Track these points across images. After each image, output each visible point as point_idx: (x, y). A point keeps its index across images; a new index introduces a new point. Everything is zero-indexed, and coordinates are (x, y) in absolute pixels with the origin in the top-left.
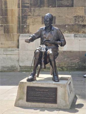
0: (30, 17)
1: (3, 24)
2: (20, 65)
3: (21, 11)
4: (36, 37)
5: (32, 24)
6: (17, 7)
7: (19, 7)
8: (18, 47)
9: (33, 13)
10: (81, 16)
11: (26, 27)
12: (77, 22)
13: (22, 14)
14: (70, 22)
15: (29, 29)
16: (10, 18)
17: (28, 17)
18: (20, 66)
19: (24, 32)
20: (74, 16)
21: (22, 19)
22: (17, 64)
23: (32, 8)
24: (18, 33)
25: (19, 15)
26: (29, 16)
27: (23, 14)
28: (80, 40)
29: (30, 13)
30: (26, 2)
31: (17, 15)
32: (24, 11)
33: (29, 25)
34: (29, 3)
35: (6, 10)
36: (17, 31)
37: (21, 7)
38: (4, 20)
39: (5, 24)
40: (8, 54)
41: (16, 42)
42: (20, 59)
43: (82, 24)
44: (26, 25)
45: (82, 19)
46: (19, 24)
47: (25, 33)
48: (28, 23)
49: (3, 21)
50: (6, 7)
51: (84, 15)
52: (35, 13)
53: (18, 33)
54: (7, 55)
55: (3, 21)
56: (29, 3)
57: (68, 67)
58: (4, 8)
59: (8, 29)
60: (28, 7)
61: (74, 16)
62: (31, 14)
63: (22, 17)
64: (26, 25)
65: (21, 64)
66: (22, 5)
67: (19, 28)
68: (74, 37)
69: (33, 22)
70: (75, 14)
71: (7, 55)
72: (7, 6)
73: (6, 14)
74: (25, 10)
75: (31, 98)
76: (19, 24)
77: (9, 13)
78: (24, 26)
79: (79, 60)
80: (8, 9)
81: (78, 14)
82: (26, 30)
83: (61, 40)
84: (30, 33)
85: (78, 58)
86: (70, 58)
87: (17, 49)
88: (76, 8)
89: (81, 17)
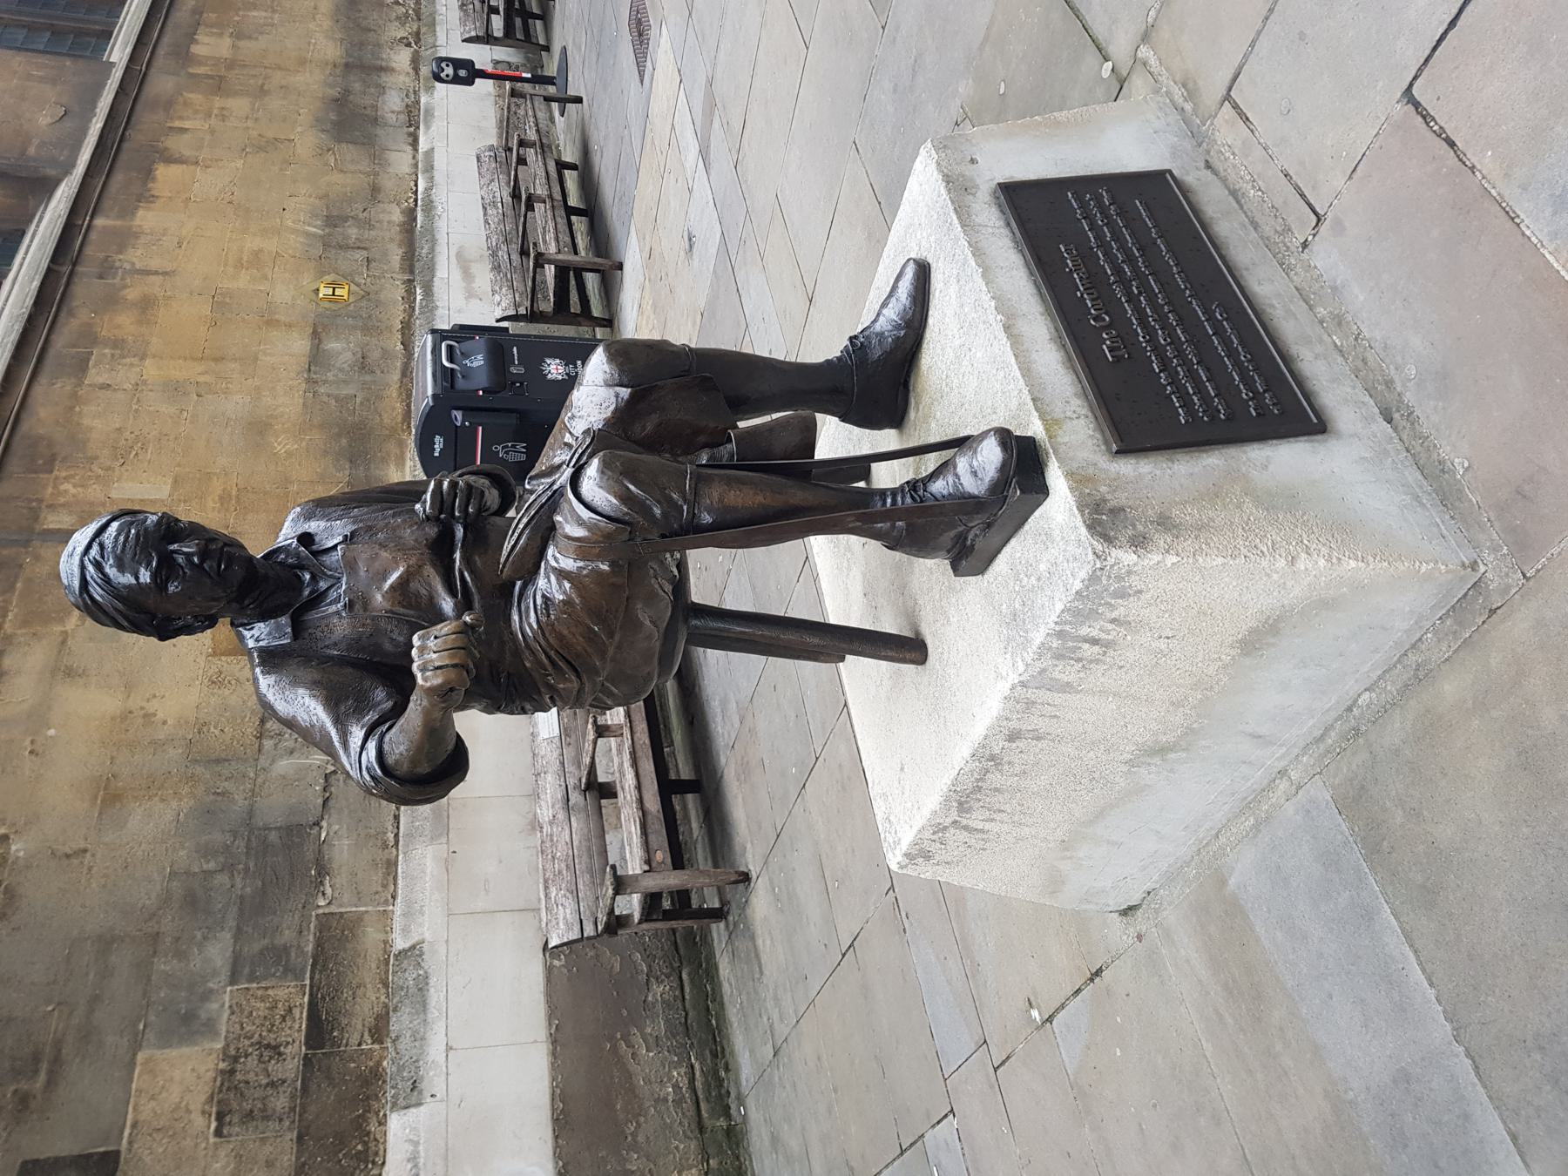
10: (222, 1065)
12: (280, 1102)
14: (269, 1164)
20: (218, 1133)
28: (449, 1048)
43: (296, 1049)
45: (252, 1061)
51: (219, 1045)
57: (701, 1128)
61: (212, 1140)
68: (419, 1104)
70: (199, 1121)
75: (1245, 378)
79: (625, 1038)
81: (198, 1100)
85: (615, 1049)
86: (622, 1116)
88: (134, 1126)
89: (232, 1072)
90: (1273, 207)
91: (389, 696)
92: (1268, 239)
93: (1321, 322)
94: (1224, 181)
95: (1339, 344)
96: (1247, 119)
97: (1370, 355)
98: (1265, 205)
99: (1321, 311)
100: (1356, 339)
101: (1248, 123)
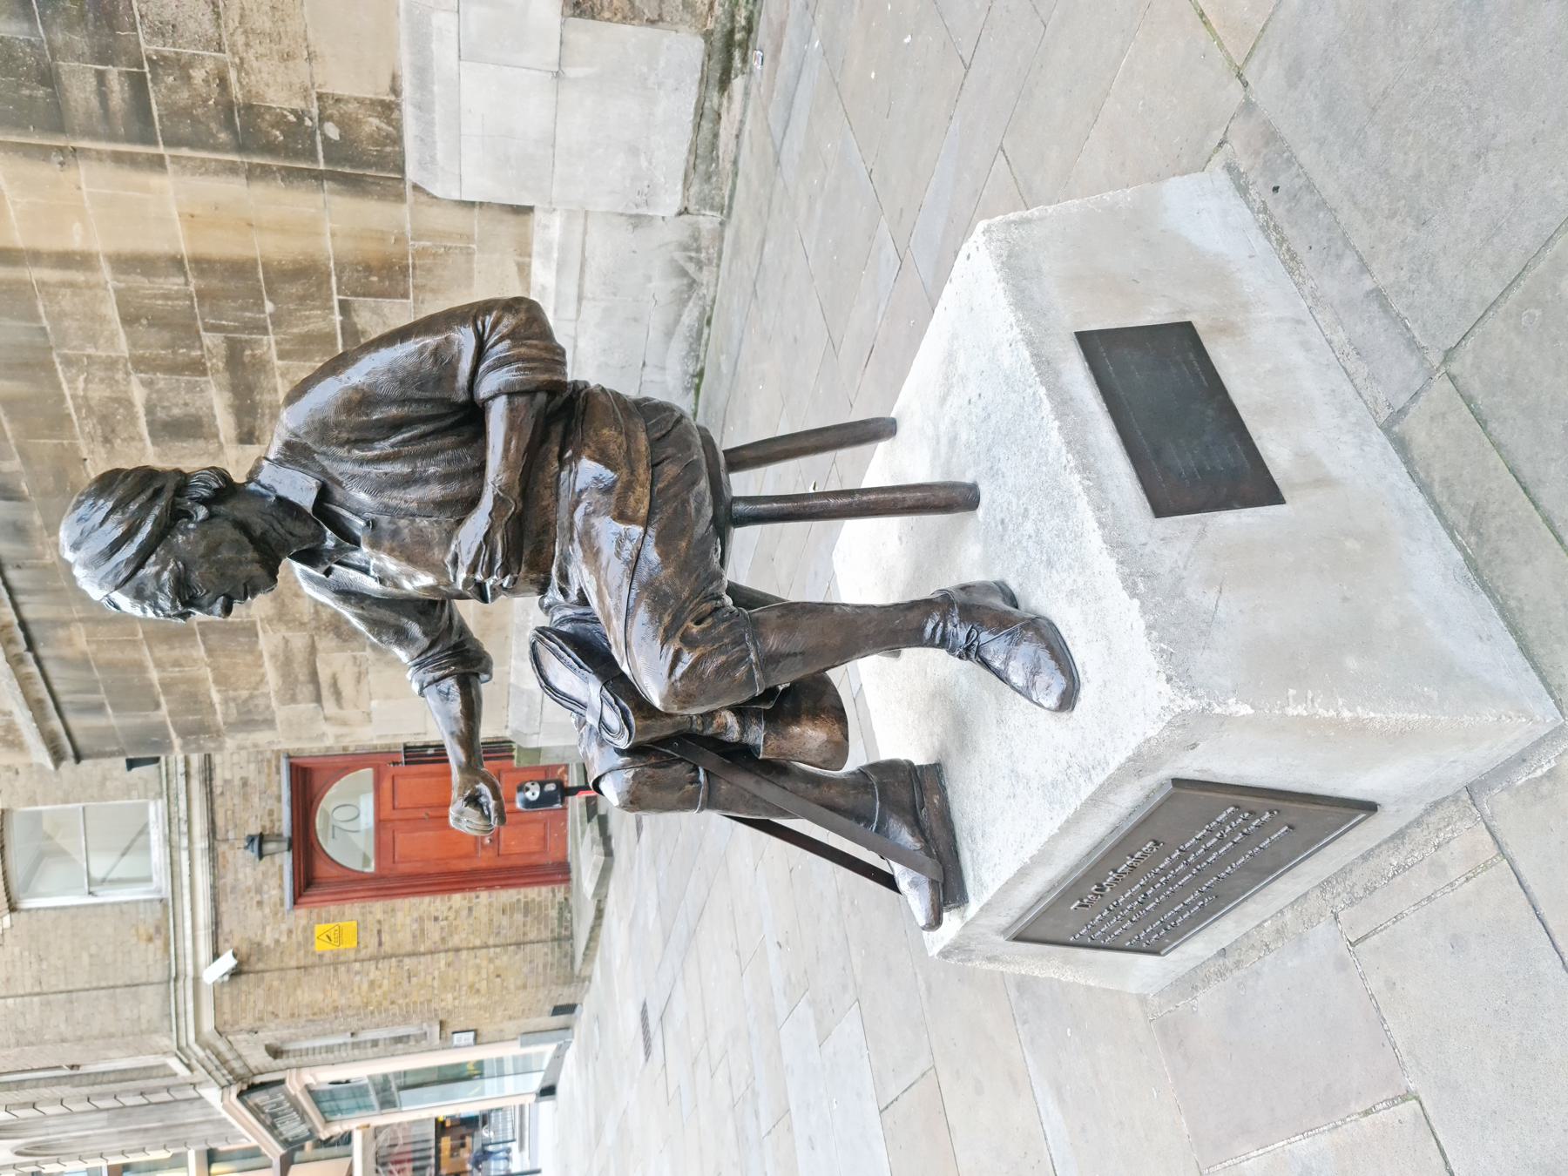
0: (232, 76)
1: (329, 298)
2: (676, 210)
3: (185, 152)
4: (425, 642)
5: (303, 66)
6: (155, 180)
7: (157, 163)
8: (524, 211)
9: (192, 43)
11: (340, 124)
13: (215, 148)
15: (361, 102)
16: (266, 247)
17: (236, 92)
18: (680, 214)
19: (388, 149)
21: (270, 149)
22: (673, 232)
23: (144, 45)
24: (400, 197)
25: (232, 169)
26: (223, 82)
27: (213, 136)
29: (198, 75)
30: (95, 102)
31: (233, 189)
32: (185, 129)
33: (320, 97)
34: (101, 77)
35: (203, 265)
36: (382, 197)
37: (151, 150)
38: (296, 289)
39: (329, 282)
40: (580, 286)
41: (476, 223)
42: (620, 210)
44: (322, 120)
46: (316, 178)
47: (397, 140)
48: (298, 104)
49: (302, 299)
50: (177, 263)
52: (192, 25)
53: (400, 197)
54: (580, 298)
55: (302, 299)
56: (101, 77)
58: (181, 280)
59: (369, 269)
60: (138, 84)
62: (210, 65)
63: (241, 148)
64: (322, 120)
65: (670, 201)
66: (129, 139)
67: (354, 184)
69: (287, 57)
71: (588, 293)
72: (159, 258)
73: (240, 269)
74: (175, 113)
76: (319, 176)
77: (223, 245)
78: (327, 140)
80: (184, 249)
82: (367, 129)
83: (462, 397)
84: (395, 90)
87: (538, 215)
90: (1375, 888)
91: (425, 634)
92: (1351, 870)
93: (1281, 911)
94: (1418, 822)
95: (1266, 925)
96: (1467, 879)
97: (1254, 954)
98: (1379, 878)
99: (1288, 915)
100: (1266, 945)
101: (1463, 879)
